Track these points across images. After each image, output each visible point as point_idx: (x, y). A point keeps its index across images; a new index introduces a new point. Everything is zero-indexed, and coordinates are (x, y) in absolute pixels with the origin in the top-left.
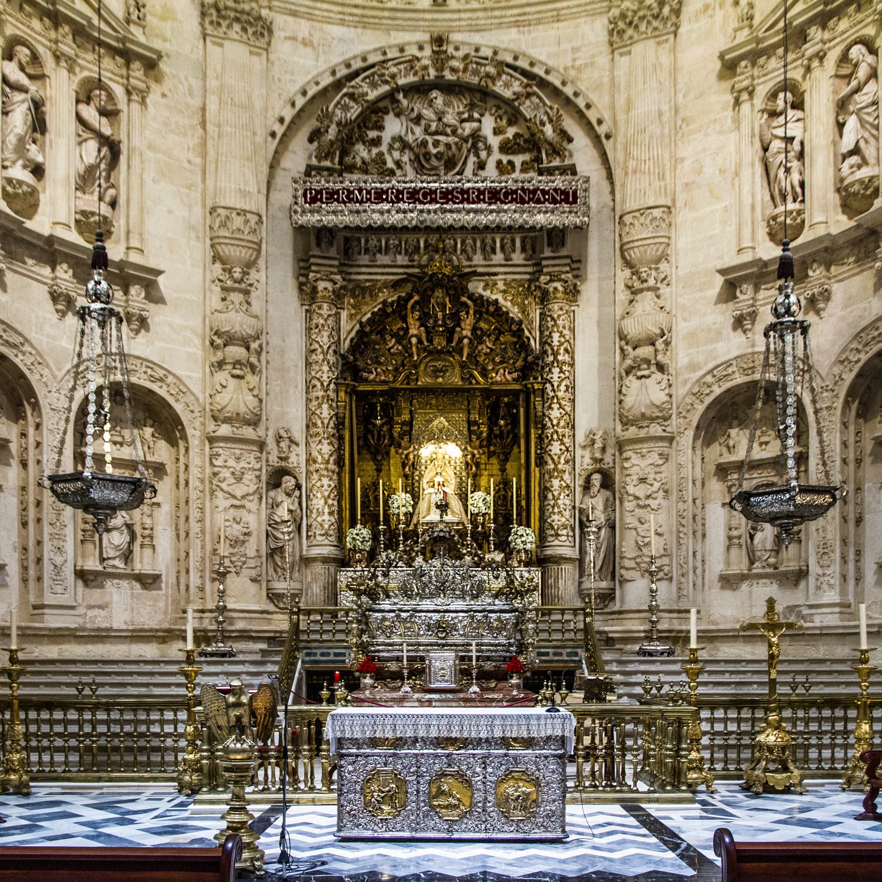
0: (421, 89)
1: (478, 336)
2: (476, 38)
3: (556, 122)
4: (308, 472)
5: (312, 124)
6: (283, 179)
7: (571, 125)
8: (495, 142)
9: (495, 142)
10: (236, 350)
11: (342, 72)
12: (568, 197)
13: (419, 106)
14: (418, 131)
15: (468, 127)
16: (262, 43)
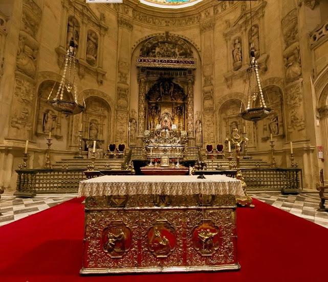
0: (163, 43)
1: (174, 92)
2: (175, 33)
3: (190, 49)
4: (138, 119)
5: (141, 47)
6: (134, 58)
7: (193, 50)
8: (178, 53)
9: (178, 53)
10: (122, 93)
11: (148, 38)
12: (192, 63)
13: (163, 45)
14: (163, 51)
15: (173, 50)
16: (131, 29)
